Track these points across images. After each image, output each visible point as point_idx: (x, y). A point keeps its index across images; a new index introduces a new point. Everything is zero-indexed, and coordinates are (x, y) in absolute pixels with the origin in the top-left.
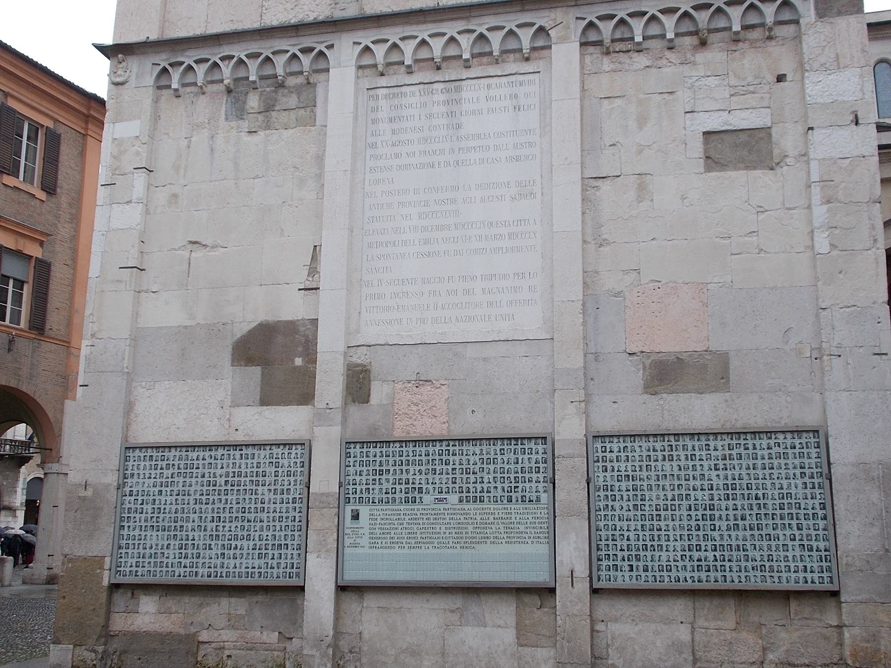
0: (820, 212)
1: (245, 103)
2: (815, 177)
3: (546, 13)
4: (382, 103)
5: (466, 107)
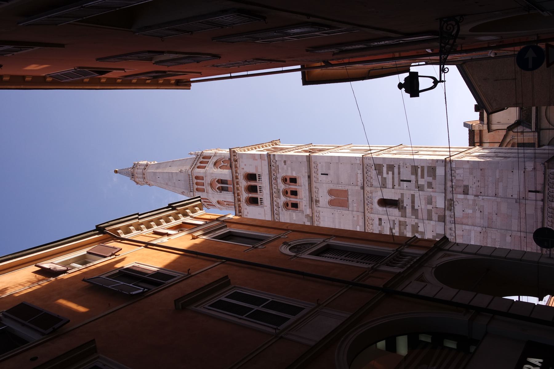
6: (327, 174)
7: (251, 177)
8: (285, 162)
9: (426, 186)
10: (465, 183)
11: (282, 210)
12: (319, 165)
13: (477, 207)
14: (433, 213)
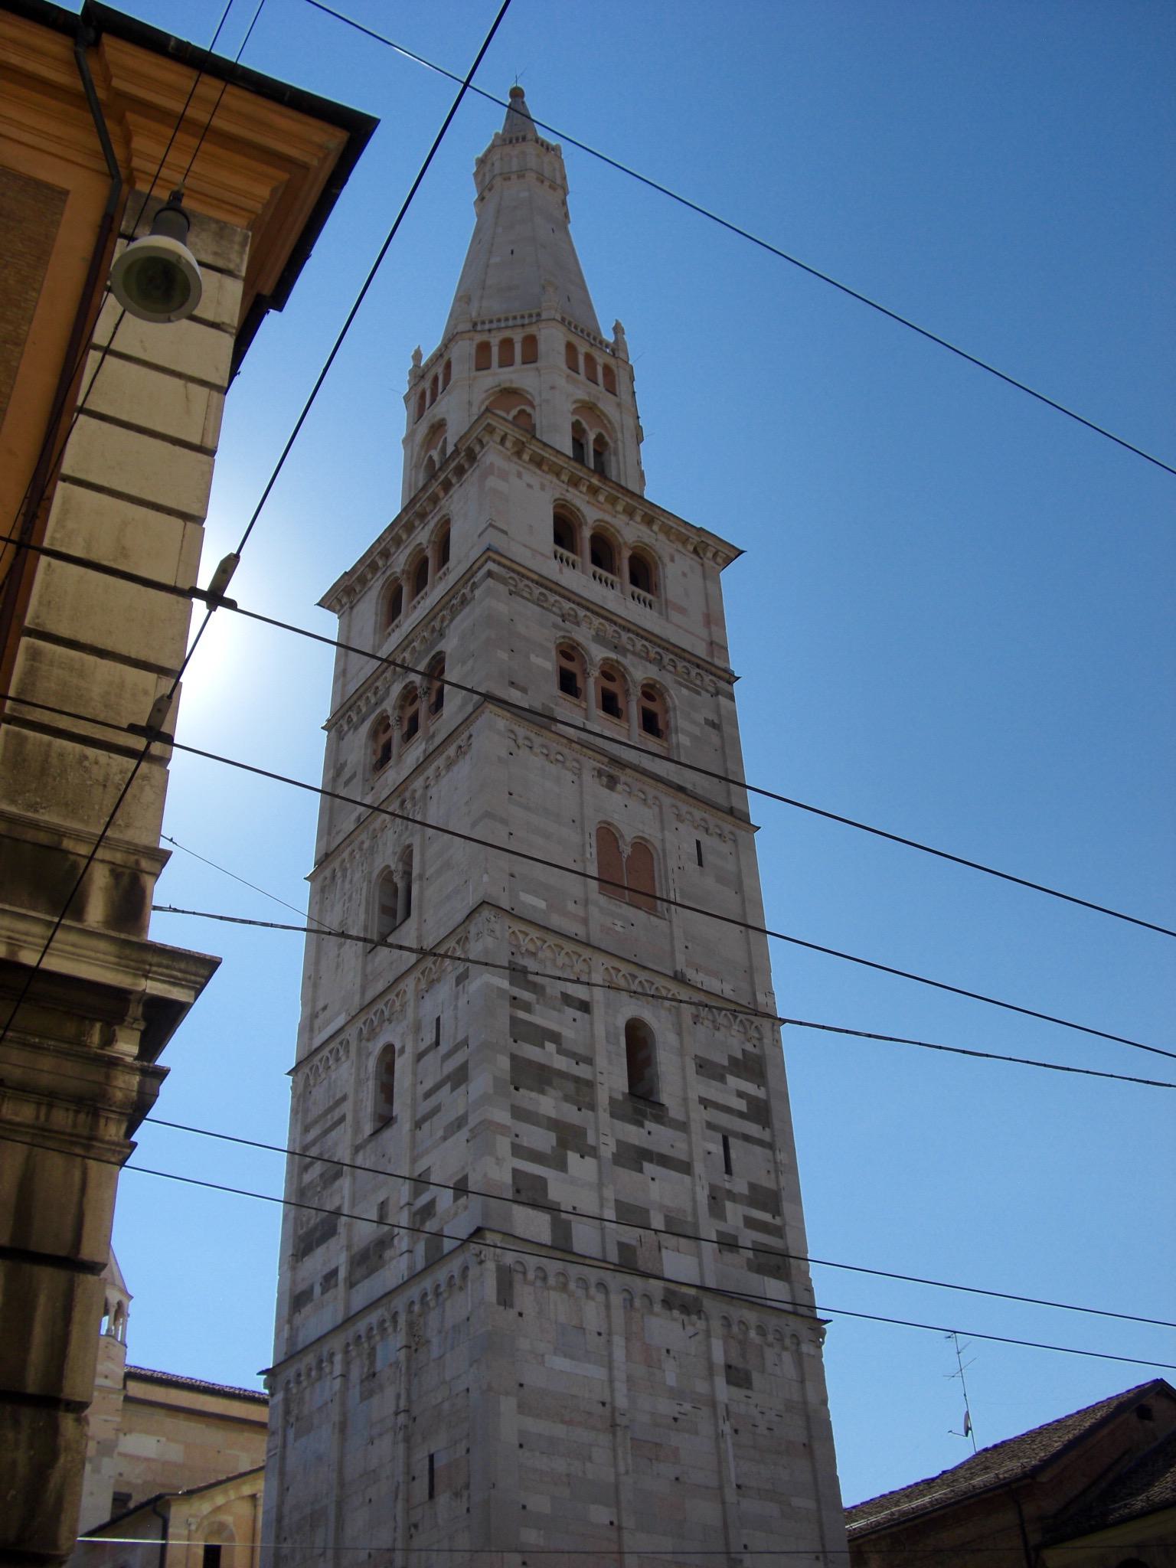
6: (700, 864)
7: (643, 574)
10: (756, 1377)
11: (555, 626)
13: (687, 1407)
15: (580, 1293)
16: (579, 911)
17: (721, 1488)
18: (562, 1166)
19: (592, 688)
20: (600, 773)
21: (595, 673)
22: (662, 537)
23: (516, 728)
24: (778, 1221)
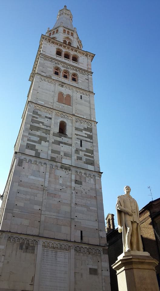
0: (104, 283)
1: (23, 247)
2: (103, 278)
3: (70, 244)
4: (45, 252)
5: (58, 256)
6: (81, 98)
7: (75, 59)
8: (87, 79)
9: (78, 155)
10: (83, 183)
11: (53, 64)
12: (87, 97)
13: (64, 187)
14: (57, 155)
15: (40, 165)
16: (52, 104)
17: (71, 204)
18: (40, 143)
19: (61, 74)
20: (60, 85)
21: (62, 72)
22: (79, 53)
23: (42, 78)
24: (93, 155)
